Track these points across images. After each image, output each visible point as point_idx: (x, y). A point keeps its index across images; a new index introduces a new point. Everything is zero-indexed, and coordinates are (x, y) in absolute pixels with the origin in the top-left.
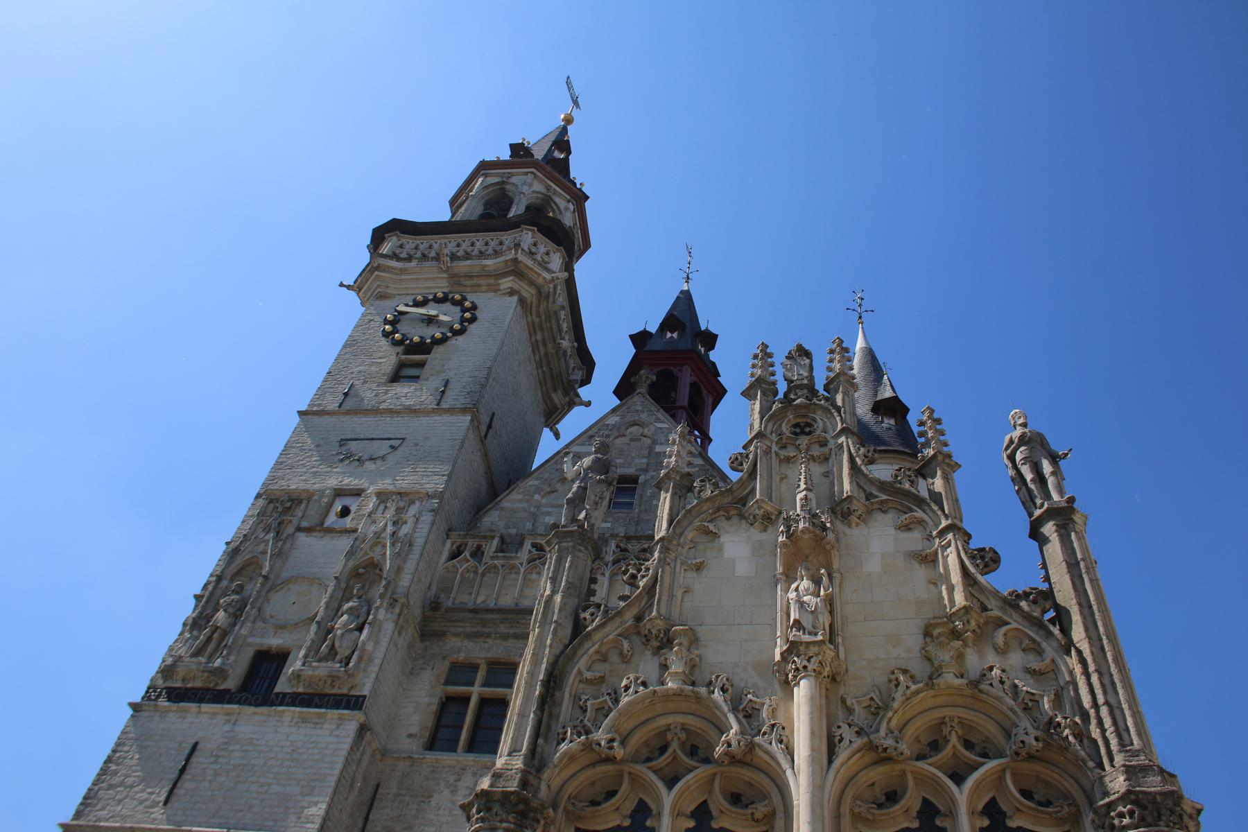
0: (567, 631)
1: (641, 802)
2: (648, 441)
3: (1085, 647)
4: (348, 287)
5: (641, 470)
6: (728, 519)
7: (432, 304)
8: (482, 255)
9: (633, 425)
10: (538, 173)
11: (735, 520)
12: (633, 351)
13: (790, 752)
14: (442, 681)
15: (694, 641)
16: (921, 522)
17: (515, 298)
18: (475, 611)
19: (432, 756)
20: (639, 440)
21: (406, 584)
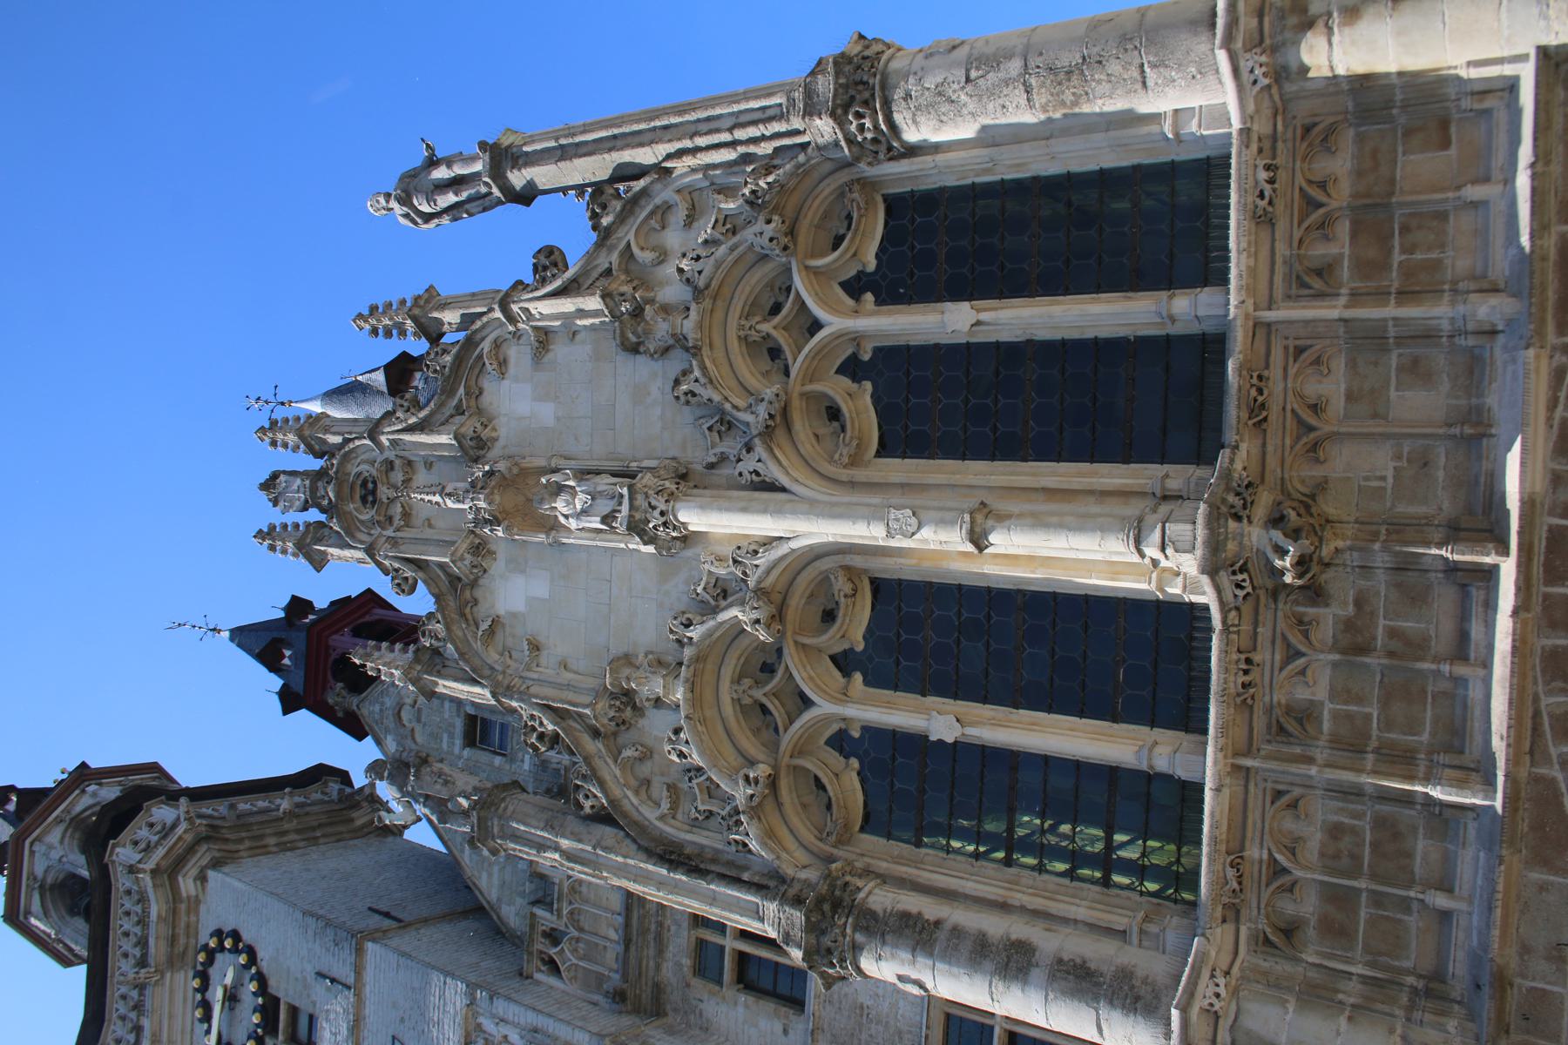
0: (608, 831)
1: (830, 742)
2: (421, 699)
3: (663, 149)
5: (458, 711)
6: (476, 602)
7: (208, 995)
8: (143, 921)
9: (400, 718)
11: (478, 593)
12: (304, 711)
13: (769, 542)
14: (717, 988)
15: (627, 659)
16: (497, 345)
17: (211, 874)
18: (627, 942)
19: (811, 1004)
20: (419, 710)
21: (587, 1037)
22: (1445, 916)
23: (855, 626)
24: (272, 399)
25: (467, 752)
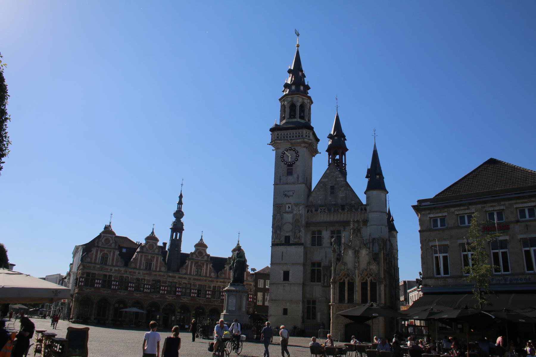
4: (269, 144)
10: (300, 96)
17: (305, 148)
23: (351, 281)
25: (329, 187)
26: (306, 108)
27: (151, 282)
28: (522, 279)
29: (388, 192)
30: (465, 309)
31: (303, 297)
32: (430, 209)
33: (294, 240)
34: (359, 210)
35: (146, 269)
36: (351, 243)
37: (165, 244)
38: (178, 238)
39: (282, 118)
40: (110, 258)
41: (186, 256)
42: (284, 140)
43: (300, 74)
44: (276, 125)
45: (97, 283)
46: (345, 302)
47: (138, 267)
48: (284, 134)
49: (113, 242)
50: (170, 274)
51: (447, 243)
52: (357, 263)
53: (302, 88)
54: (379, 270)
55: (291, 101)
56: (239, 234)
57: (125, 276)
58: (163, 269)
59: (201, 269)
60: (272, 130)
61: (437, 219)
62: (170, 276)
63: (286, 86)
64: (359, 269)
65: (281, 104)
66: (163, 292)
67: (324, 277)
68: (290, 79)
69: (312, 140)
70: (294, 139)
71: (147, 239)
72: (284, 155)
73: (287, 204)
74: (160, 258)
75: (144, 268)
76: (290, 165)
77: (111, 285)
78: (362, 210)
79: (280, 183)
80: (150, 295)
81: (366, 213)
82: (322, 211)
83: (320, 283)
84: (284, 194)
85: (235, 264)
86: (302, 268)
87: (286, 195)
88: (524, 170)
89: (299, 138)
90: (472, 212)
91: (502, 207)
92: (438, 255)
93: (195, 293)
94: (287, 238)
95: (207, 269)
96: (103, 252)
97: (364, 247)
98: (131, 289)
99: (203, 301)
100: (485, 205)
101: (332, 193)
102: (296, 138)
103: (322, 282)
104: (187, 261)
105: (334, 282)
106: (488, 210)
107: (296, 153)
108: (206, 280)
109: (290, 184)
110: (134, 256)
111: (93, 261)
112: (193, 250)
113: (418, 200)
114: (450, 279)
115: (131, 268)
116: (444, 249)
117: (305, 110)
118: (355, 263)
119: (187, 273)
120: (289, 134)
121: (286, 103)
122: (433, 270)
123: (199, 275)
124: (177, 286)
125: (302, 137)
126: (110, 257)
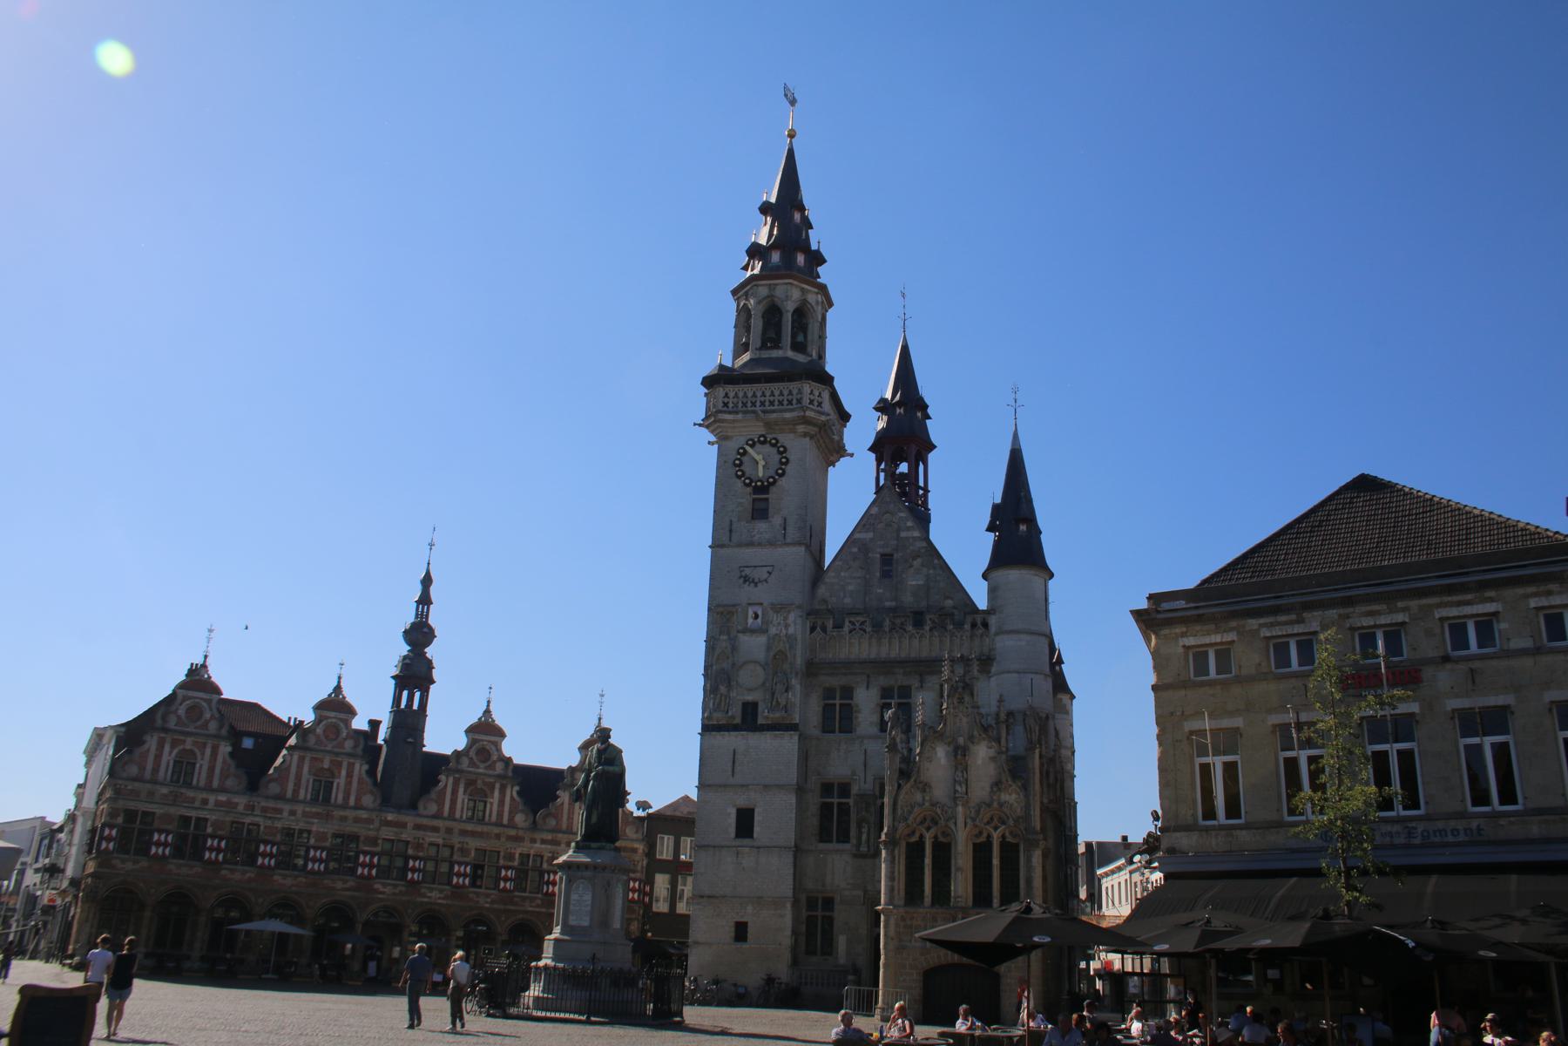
4: (700, 425)
10: (795, 283)
17: (808, 439)
20: (891, 525)
22: (911, 941)
23: (941, 839)
24: (1017, 405)
25: (878, 556)
26: (811, 321)
27: (330, 840)
28: (1458, 830)
29: (1052, 575)
30: (1321, 918)
31: (794, 889)
32: (1184, 621)
33: (771, 715)
34: (966, 626)
35: (315, 800)
36: (945, 724)
37: (375, 724)
38: (415, 706)
39: (741, 347)
40: (201, 766)
41: (439, 761)
42: (745, 412)
43: (797, 216)
44: (721, 367)
45: (158, 844)
46: (923, 902)
47: (289, 794)
48: (745, 395)
49: (212, 716)
50: (390, 817)
51: (1238, 722)
52: (960, 785)
53: (801, 259)
54: (1027, 806)
55: (768, 297)
56: (602, 696)
57: (247, 820)
58: (368, 800)
59: (485, 802)
60: (709, 382)
61: (1206, 653)
62: (388, 821)
63: (755, 251)
64: (967, 802)
65: (738, 306)
66: (366, 871)
67: (859, 827)
68: (765, 231)
69: (828, 415)
70: (774, 411)
71: (321, 707)
72: (745, 459)
73: (750, 604)
74: (360, 768)
75: (309, 797)
76: (762, 489)
77: (205, 848)
78: (974, 625)
79: (730, 540)
80: (326, 881)
81: (987, 636)
82: (855, 629)
83: (847, 846)
84: (741, 577)
85: (591, 782)
86: (793, 799)
87: (746, 579)
88: (1459, 509)
89: (790, 407)
90: (1312, 630)
91: (1400, 618)
92: (1209, 760)
93: (465, 875)
94: (750, 709)
95: (502, 802)
96: (181, 747)
97: (984, 736)
98: (266, 861)
99: (489, 900)
100: (1351, 610)
101: (886, 574)
102: (780, 407)
103: (854, 841)
104: (442, 777)
105: (892, 843)
106: (1359, 625)
107: (780, 453)
108: (498, 836)
109: (760, 544)
110: (279, 760)
111: (148, 775)
112: (460, 743)
113: (1150, 594)
114: (1244, 832)
115: (267, 797)
116: (1228, 741)
117: (810, 326)
118: (955, 787)
119: (442, 813)
120: (759, 394)
121: (752, 301)
122: (1194, 801)
123: (478, 820)
124: (410, 852)
125: (799, 405)
126: (202, 764)
